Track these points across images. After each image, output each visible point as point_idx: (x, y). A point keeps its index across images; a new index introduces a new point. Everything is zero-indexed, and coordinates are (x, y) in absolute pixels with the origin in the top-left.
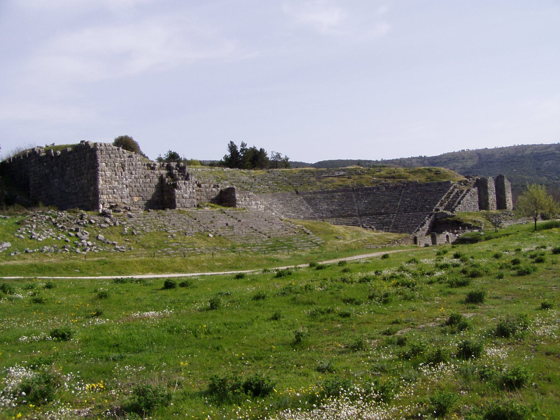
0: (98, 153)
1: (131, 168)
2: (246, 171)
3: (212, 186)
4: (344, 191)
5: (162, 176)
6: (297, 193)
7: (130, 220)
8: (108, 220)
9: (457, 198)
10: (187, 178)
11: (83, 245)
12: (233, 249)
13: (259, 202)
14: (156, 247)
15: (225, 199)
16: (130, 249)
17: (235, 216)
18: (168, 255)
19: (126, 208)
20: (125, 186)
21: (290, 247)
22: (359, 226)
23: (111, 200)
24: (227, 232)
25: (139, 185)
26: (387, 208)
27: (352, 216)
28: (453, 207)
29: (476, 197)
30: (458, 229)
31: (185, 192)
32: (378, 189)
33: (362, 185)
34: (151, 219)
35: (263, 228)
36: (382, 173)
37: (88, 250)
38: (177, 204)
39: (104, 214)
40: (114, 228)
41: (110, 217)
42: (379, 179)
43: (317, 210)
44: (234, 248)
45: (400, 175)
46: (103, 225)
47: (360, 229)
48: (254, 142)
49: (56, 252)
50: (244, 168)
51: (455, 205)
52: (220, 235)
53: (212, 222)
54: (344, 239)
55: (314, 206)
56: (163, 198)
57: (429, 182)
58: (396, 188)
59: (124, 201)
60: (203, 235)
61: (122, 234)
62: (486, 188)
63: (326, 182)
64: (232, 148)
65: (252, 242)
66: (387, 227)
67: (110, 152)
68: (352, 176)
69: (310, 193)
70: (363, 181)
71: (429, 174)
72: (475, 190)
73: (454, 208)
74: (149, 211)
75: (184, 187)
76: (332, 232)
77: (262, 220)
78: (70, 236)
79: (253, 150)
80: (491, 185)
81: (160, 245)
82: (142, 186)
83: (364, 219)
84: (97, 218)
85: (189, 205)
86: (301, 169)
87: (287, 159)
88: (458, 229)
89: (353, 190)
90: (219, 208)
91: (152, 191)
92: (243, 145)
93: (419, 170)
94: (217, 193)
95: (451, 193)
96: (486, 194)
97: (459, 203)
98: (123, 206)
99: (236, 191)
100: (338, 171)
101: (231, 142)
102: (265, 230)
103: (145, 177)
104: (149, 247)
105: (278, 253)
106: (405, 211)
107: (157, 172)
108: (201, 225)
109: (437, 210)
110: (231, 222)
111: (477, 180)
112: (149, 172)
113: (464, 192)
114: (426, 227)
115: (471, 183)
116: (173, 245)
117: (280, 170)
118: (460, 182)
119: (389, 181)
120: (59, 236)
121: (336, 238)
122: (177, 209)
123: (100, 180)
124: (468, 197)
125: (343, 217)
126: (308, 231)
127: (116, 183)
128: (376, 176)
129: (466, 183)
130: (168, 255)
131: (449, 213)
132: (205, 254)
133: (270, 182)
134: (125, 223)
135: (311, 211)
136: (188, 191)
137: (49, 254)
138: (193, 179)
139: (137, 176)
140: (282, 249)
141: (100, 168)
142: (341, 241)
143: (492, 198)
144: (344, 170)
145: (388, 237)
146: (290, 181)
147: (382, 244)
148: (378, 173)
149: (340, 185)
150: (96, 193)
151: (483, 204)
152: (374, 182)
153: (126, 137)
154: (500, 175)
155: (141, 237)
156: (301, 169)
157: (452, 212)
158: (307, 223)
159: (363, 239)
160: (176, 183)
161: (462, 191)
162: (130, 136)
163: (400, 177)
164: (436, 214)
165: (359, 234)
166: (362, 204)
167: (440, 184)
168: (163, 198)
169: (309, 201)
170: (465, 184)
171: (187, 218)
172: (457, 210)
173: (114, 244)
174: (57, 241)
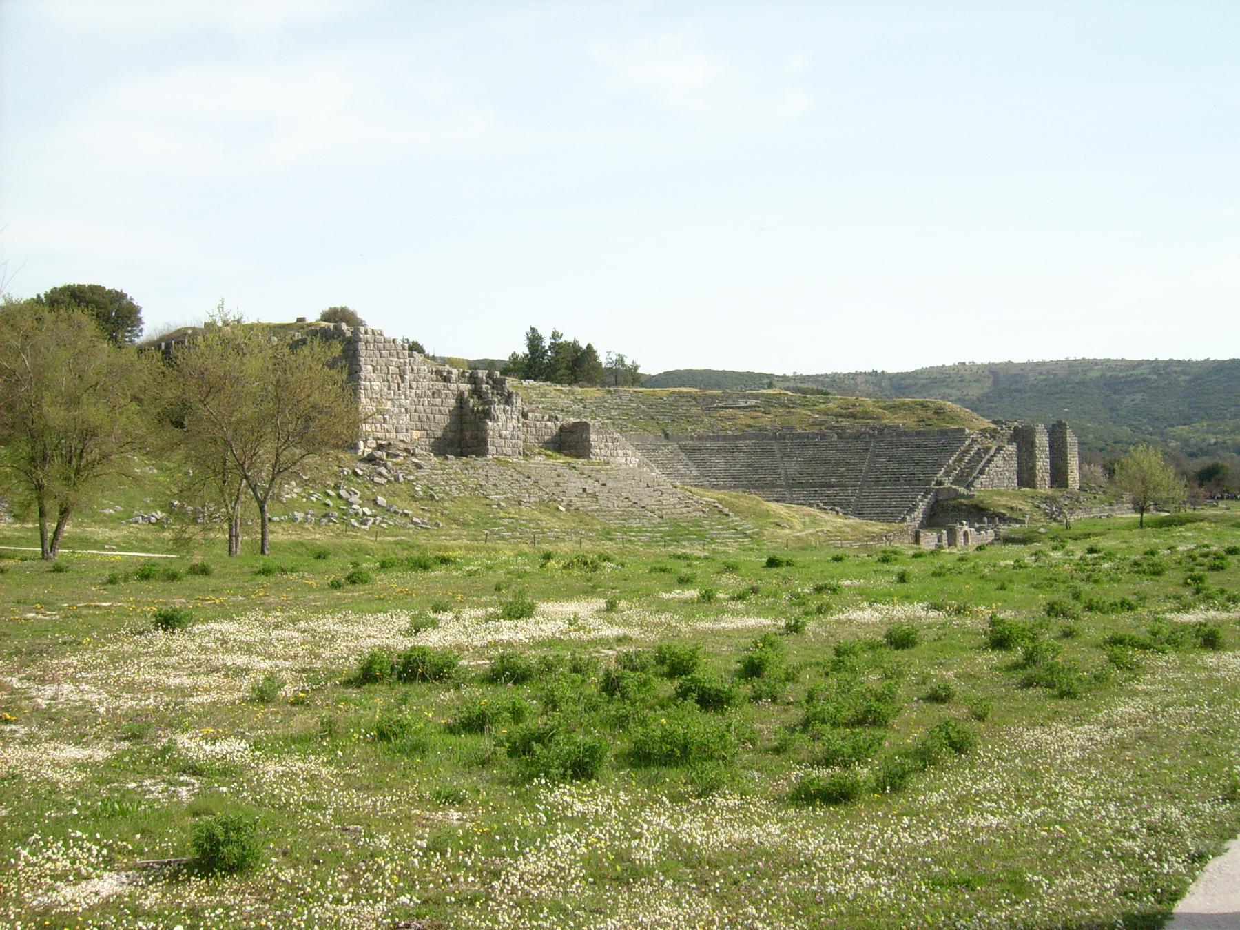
0: (361, 346)
2: (566, 388)
3: (547, 417)
4: (757, 436)
5: (462, 394)
6: (667, 436)
7: (419, 474)
8: (384, 471)
9: (979, 462)
10: (508, 399)
11: (357, 514)
12: (607, 534)
13: (629, 452)
14: (476, 524)
15: (570, 442)
16: (437, 525)
17: (593, 474)
18: (503, 538)
19: (406, 450)
21: (702, 538)
22: (811, 505)
23: (379, 435)
24: (587, 504)
26: (842, 475)
27: (774, 486)
29: (1014, 462)
30: (981, 521)
31: (503, 426)
32: (823, 436)
33: (793, 428)
34: (455, 473)
35: (646, 501)
36: (830, 405)
37: (370, 523)
38: (490, 448)
39: (371, 459)
40: (397, 485)
41: (385, 466)
42: (824, 418)
43: (705, 473)
44: (609, 533)
45: (867, 413)
46: (377, 479)
47: (814, 511)
48: (577, 333)
49: (318, 523)
50: (559, 383)
52: (577, 509)
53: (558, 485)
54: (791, 528)
55: (700, 463)
56: (464, 436)
58: (857, 437)
59: (401, 437)
60: (548, 505)
61: (413, 498)
62: (1032, 444)
63: (722, 419)
64: (534, 340)
65: (635, 524)
67: (381, 345)
68: (772, 410)
69: (692, 438)
70: (794, 421)
72: (1012, 448)
74: (447, 459)
75: (502, 416)
76: (767, 514)
77: (642, 484)
78: (328, 495)
79: (574, 347)
80: (1042, 440)
81: (483, 521)
82: (428, 410)
83: (797, 493)
84: (362, 465)
85: (509, 451)
86: (671, 389)
87: (636, 368)
88: (981, 521)
89: (774, 437)
90: (562, 459)
91: (444, 420)
92: (555, 335)
93: (904, 404)
94: (555, 431)
95: (967, 451)
96: (1032, 456)
97: (982, 472)
98: (402, 446)
99: (591, 430)
100: (744, 397)
101: (533, 329)
102: (652, 503)
103: (433, 394)
104: (465, 524)
105: (684, 547)
106: (877, 482)
107: (453, 386)
108: (541, 489)
109: (939, 483)
110: (591, 486)
111: (1016, 429)
112: (440, 385)
113: (992, 452)
114: (919, 514)
115: (1003, 435)
116: (506, 522)
117: (631, 390)
118: (983, 432)
119: (845, 422)
120: (310, 495)
121: (777, 525)
122: (490, 457)
123: (363, 396)
124: (998, 461)
126: (726, 510)
128: (819, 412)
129: (994, 434)
130: (503, 538)
131: (962, 490)
132: (564, 540)
133: (614, 413)
134: (412, 478)
135: (695, 473)
136: (510, 425)
137: (307, 525)
138: (518, 402)
139: (419, 392)
140: (689, 540)
141: (362, 374)
142: (787, 531)
143: (1042, 464)
144: (756, 397)
145: (869, 529)
146: (652, 412)
147: (859, 540)
148: (823, 406)
149: (750, 426)
150: (354, 424)
151: (1026, 477)
152: (814, 424)
154: (1060, 422)
155: (446, 504)
156: (671, 389)
157: (968, 487)
158: (720, 494)
159: (825, 529)
160: (489, 409)
161: (987, 450)
162: (351, 308)
163: (866, 415)
164: (937, 492)
165: (814, 521)
166: (792, 466)
167: (944, 433)
168: (464, 436)
169: (691, 453)
170: (992, 437)
171: (516, 476)
172: (977, 484)
173: (406, 515)
174: (309, 504)
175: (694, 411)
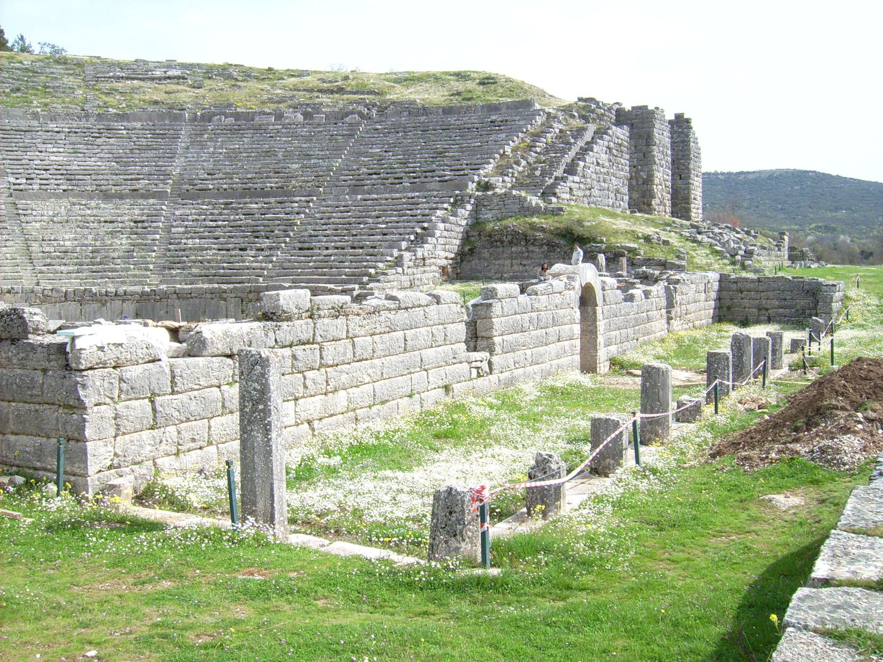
9: (564, 152)
28: (550, 181)
51: (559, 173)
57: (456, 101)
66: (267, 243)
69: (35, 116)
71: (459, 86)
73: (554, 186)
97: (571, 170)
106: (356, 188)
109: (487, 187)
113: (588, 136)
119: (325, 99)
125: (107, 196)
131: (534, 200)
149: (156, 103)
172: (562, 190)
175: (69, 81)
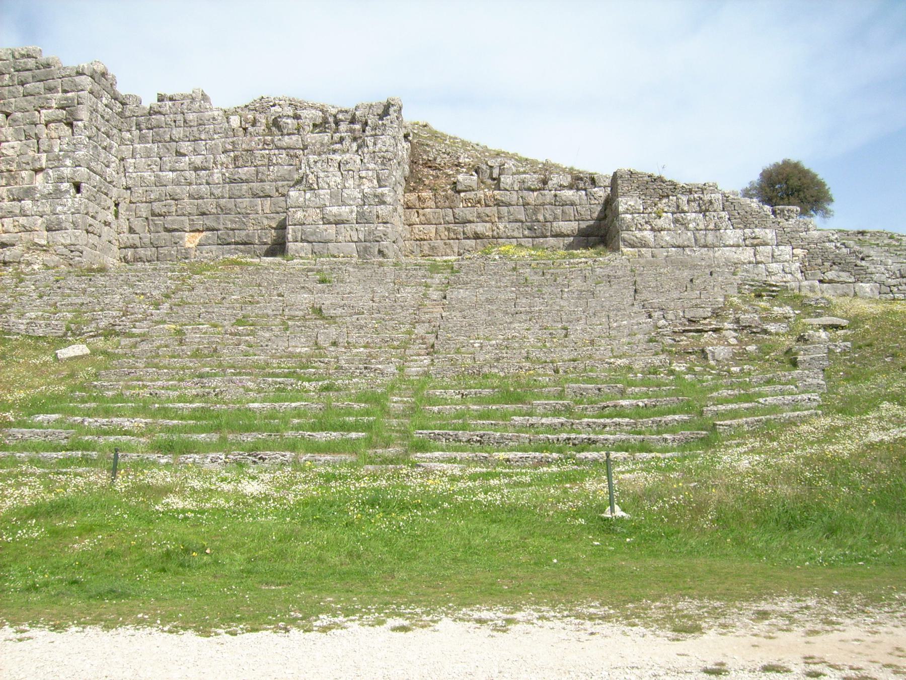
1: (178, 133)
20: (65, 186)
25: (204, 189)
127: (40, 176)
136: (352, 192)
139: (198, 160)
153: (796, 166)
162: (794, 159)
